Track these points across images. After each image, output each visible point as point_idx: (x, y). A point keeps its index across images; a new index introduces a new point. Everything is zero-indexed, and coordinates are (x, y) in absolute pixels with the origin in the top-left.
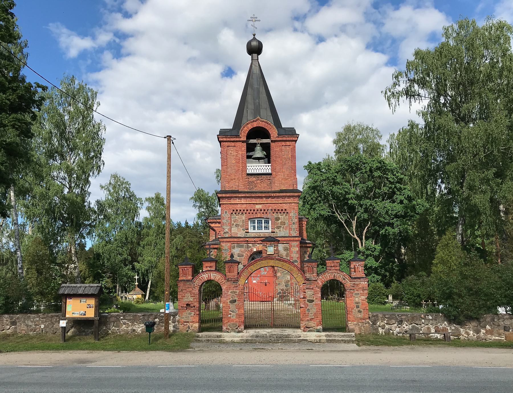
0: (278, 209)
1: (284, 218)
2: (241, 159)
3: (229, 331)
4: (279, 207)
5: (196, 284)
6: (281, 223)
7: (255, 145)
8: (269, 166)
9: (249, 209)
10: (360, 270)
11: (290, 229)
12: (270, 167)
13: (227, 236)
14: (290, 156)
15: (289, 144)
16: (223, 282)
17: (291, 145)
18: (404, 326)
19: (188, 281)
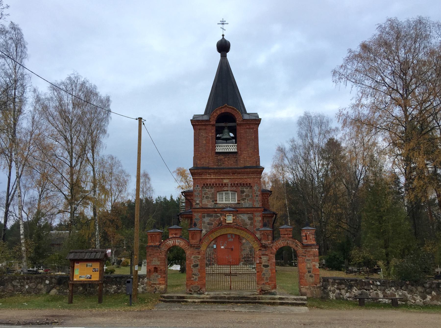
2: (211, 140)
3: (192, 293)
5: (163, 250)
6: (246, 195)
8: (235, 146)
9: (217, 182)
10: (311, 238)
12: (236, 147)
13: (198, 206)
14: (253, 137)
15: (252, 127)
16: (186, 248)
18: (354, 290)
19: (155, 246)
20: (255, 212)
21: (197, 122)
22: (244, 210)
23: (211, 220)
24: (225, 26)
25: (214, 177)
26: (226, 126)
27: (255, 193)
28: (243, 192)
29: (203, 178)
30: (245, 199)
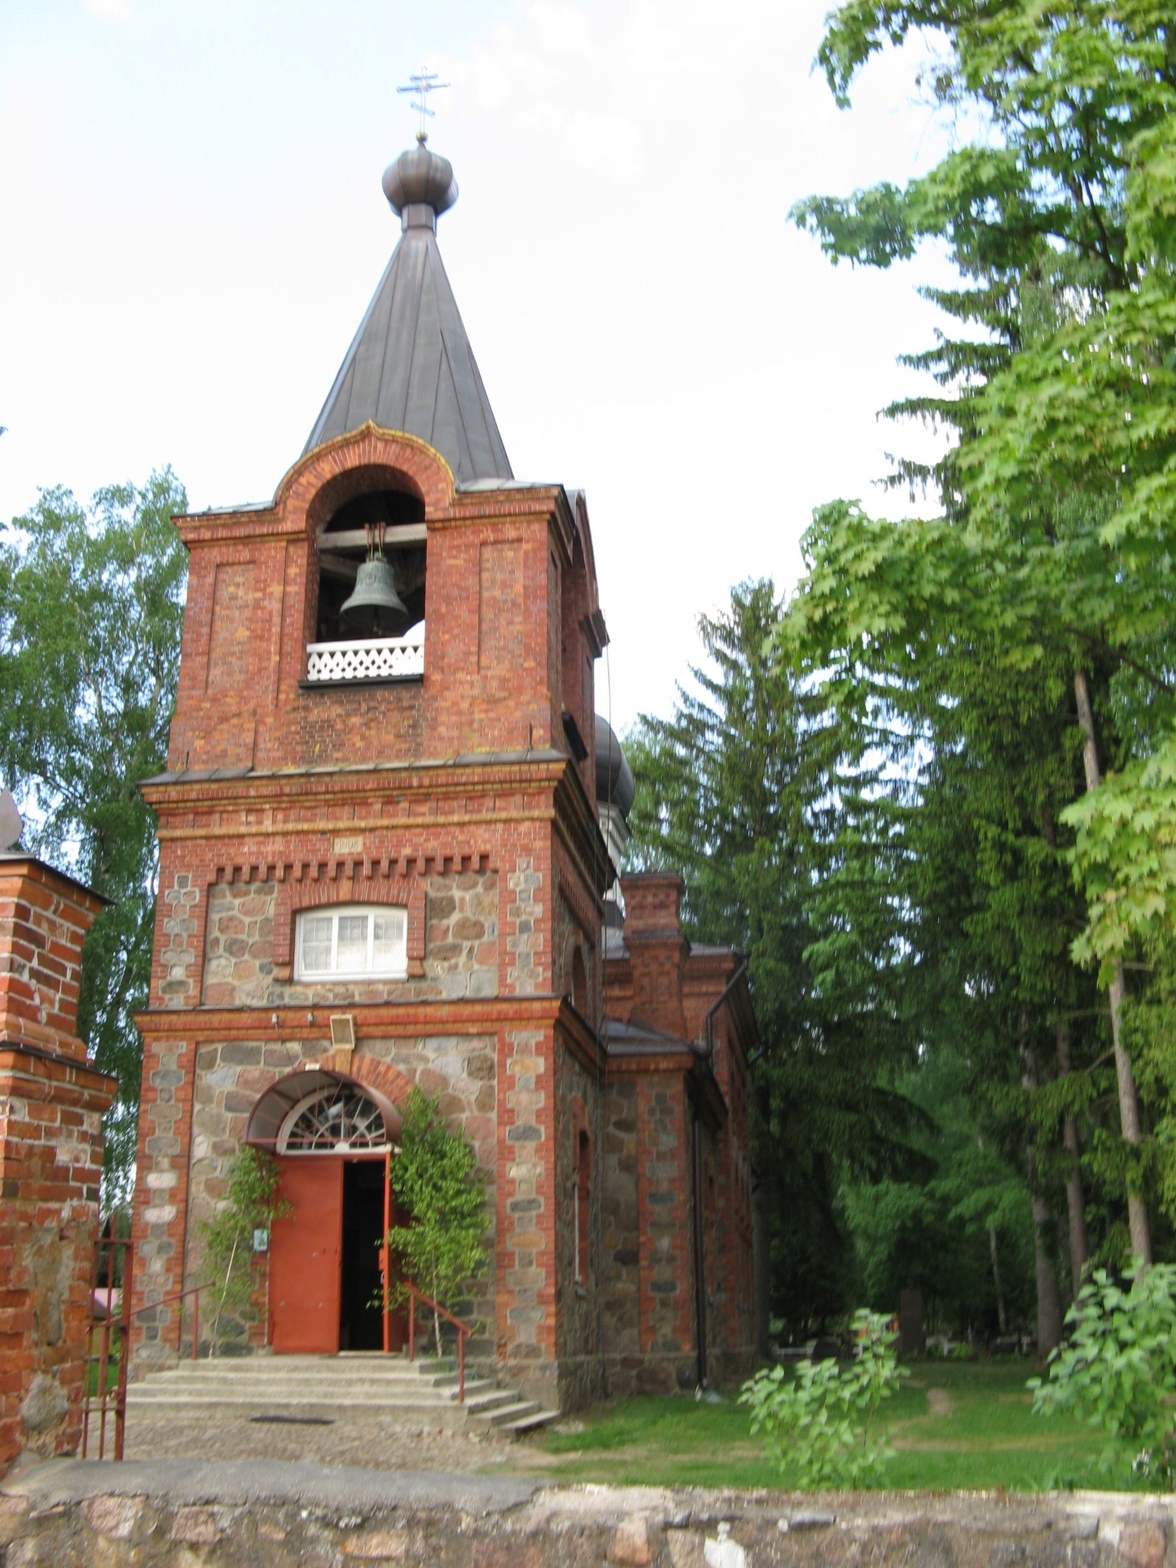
0: (448, 852)
1: (478, 900)
2: (276, 620)
4: (456, 844)
6: (462, 925)
7: (359, 555)
11: (506, 960)
14: (519, 588)
15: (511, 533)
17: (525, 536)
20: (507, 1026)
21: (208, 527)
22: (445, 1011)
23: (246, 1082)
24: (430, 99)
25: (280, 827)
26: (375, 548)
27: (517, 912)
28: (435, 908)
29: (217, 831)
30: (455, 949)
